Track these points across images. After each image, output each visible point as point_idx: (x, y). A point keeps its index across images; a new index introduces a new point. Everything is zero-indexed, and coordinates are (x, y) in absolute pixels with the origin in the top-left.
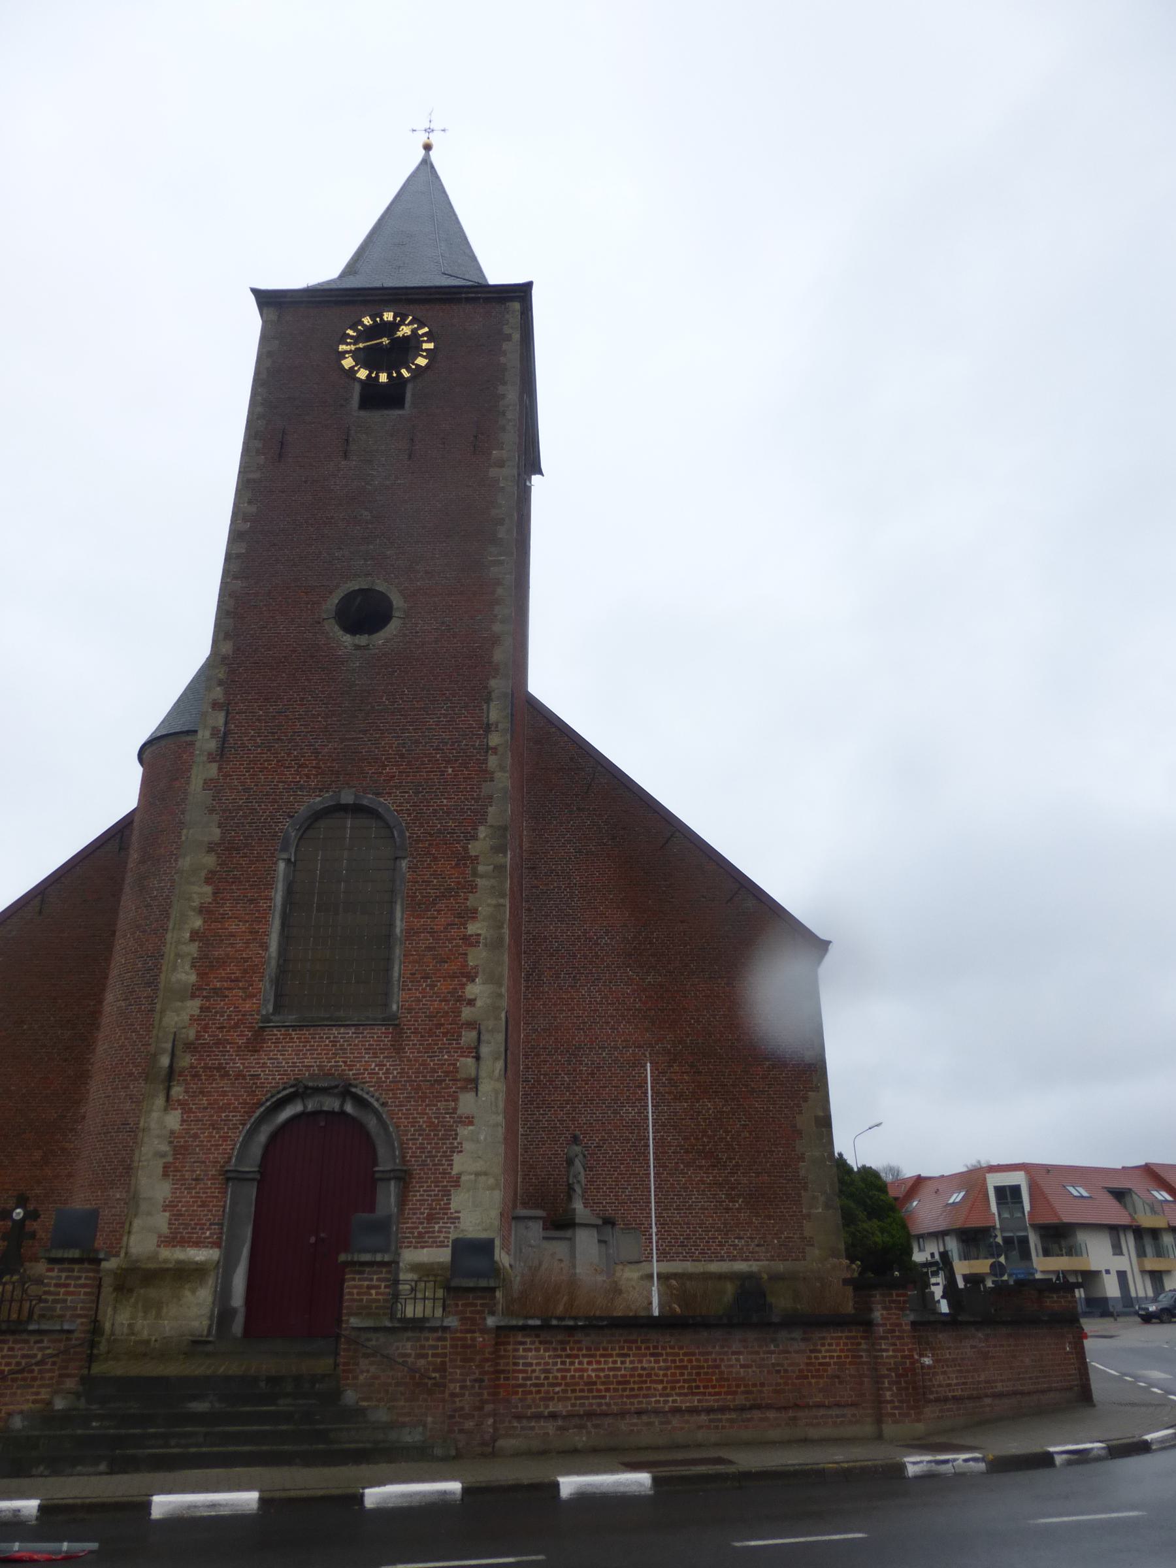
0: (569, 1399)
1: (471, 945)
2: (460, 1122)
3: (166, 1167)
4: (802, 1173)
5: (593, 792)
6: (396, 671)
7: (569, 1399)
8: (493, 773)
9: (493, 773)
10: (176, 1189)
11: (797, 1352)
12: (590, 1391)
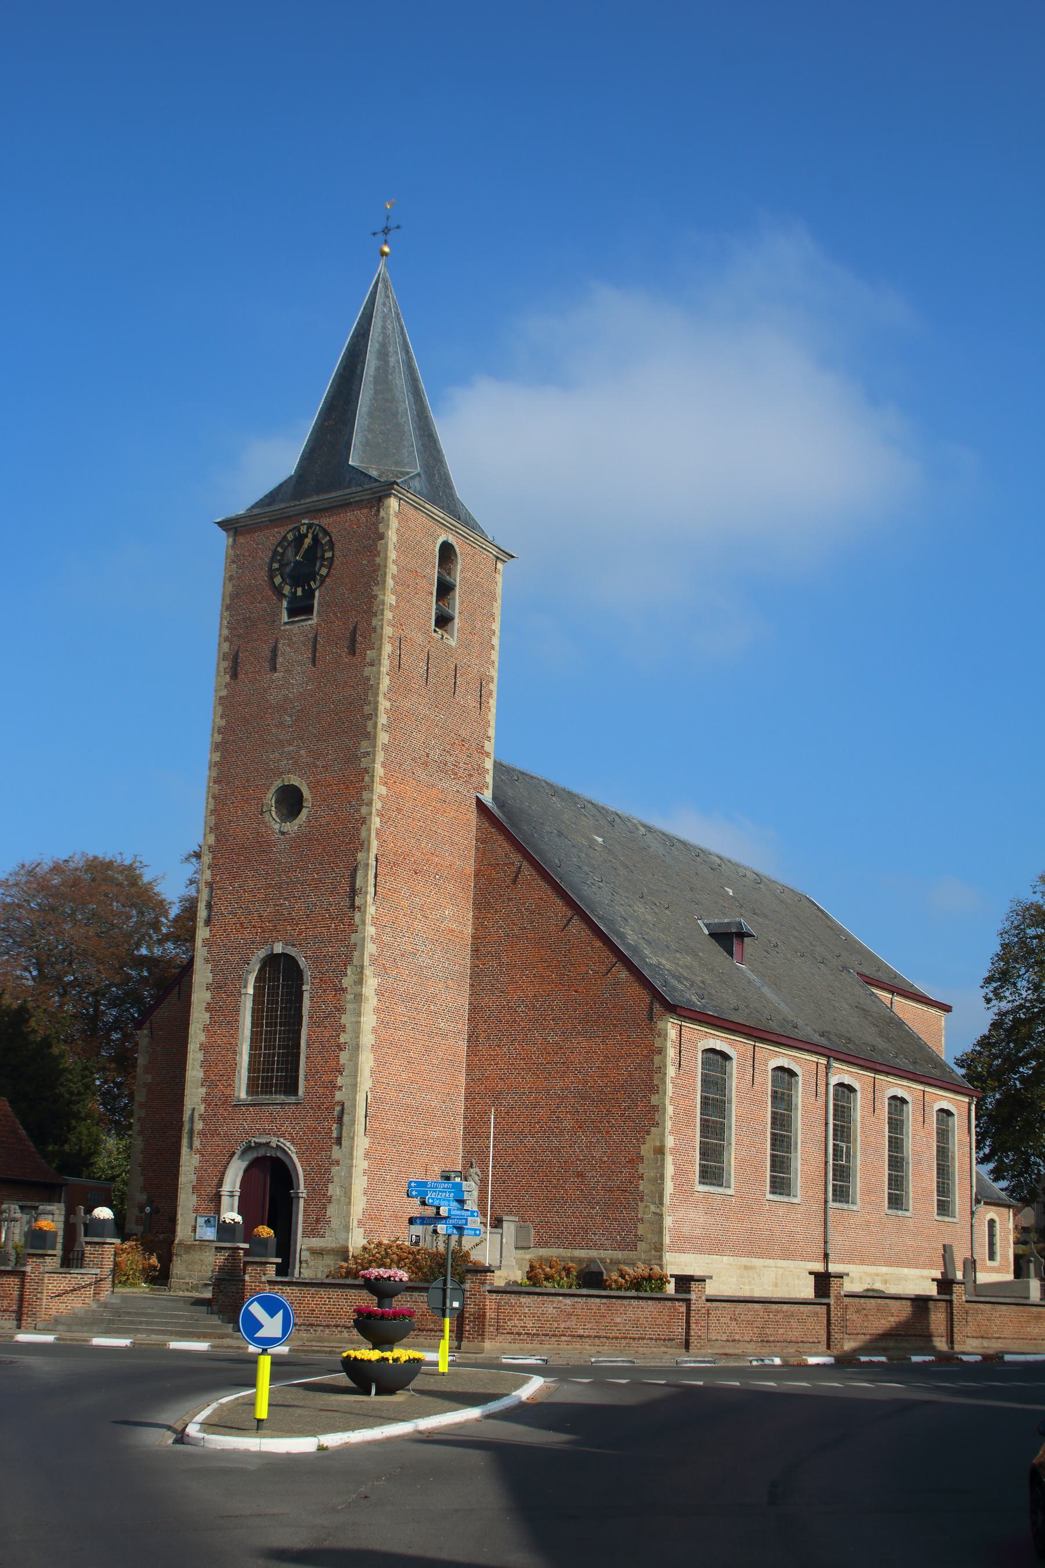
0: (301, 1317)
1: (341, 1050)
2: (333, 1164)
3: (194, 1187)
4: (641, 1188)
5: (519, 884)
6: (304, 851)
7: (301, 1317)
8: (357, 926)
9: (357, 926)
11: (422, 1302)
12: (313, 1314)
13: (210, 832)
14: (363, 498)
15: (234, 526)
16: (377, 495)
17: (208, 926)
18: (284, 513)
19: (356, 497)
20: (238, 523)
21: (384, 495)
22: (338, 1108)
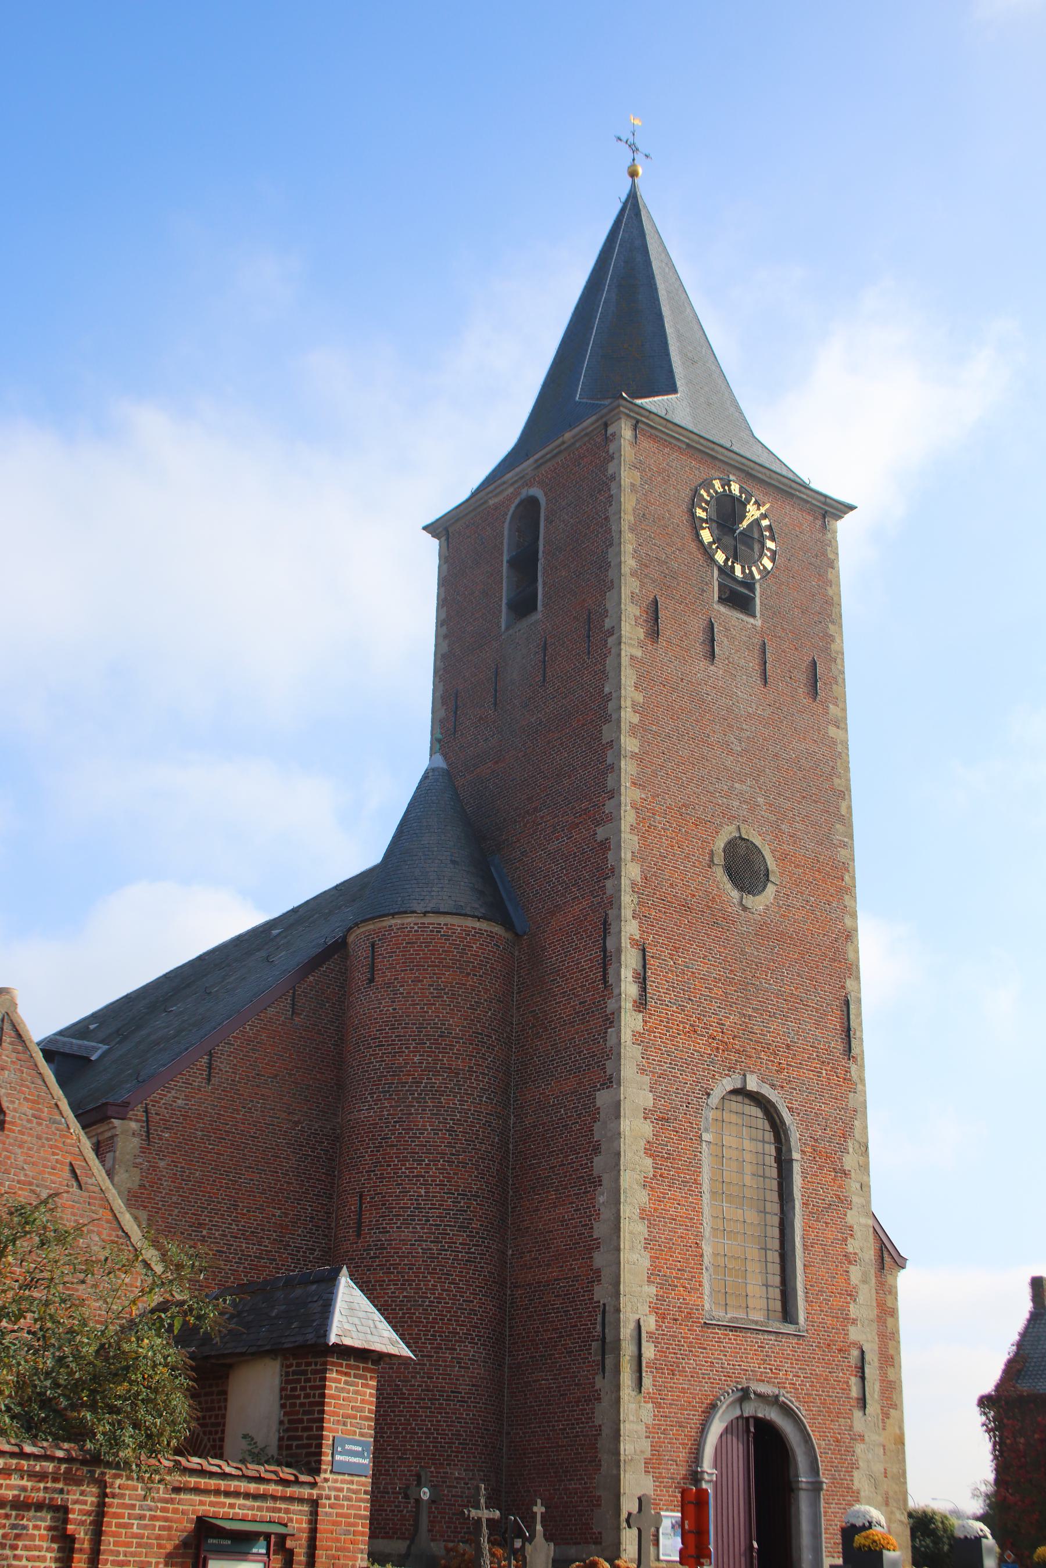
2: (856, 1440)
10: (656, 1486)
13: (632, 860)
14: (810, 500)
15: (639, 417)
16: (827, 508)
17: (640, 1011)
18: (713, 449)
19: (803, 493)
20: (647, 418)
21: (833, 513)
22: (855, 1353)
